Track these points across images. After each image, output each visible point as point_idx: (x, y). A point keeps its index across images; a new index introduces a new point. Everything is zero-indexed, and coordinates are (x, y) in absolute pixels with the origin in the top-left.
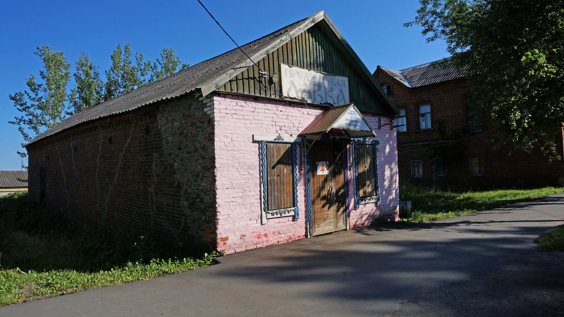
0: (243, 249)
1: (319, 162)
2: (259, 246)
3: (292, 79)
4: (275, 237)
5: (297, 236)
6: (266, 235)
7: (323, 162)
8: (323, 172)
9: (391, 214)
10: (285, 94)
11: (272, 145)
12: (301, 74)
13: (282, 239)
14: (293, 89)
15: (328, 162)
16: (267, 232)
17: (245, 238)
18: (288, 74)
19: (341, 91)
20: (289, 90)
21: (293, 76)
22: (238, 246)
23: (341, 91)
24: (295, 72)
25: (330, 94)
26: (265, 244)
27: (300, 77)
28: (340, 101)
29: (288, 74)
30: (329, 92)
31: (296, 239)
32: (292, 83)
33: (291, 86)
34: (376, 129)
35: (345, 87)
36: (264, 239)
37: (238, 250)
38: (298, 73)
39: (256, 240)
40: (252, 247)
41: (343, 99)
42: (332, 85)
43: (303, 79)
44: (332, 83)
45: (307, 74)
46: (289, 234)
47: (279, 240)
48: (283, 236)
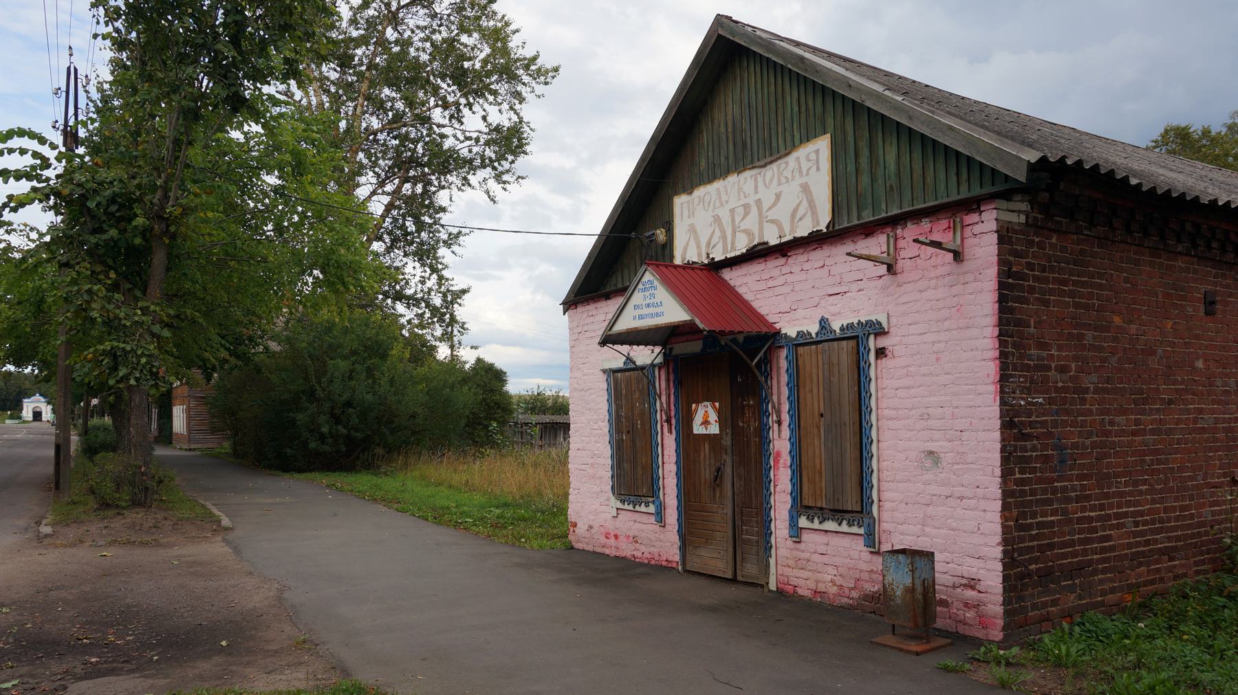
0: (590, 548)
1: (698, 403)
2: (607, 551)
5: (665, 559)
6: (616, 537)
7: (706, 403)
8: (706, 429)
9: (946, 601)
14: (692, 243)
15: (717, 404)
17: (593, 531)
18: (686, 213)
19: (806, 188)
20: (685, 249)
21: (693, 213)
23: (806, 188)
24: (696, 201)
25: (772, 215)
27: (706, 205)
28: (801, 219)
29: (686, 213)
30: (770, 209)
31: (664, 563)
34: (881, 277)
35: (818, 169)
36: (612, 541)
38: (701, 200)
39: (603, 540)
42: (779, 184)
44: (779, 180)
46: (652, 549)
47: (635, 553)
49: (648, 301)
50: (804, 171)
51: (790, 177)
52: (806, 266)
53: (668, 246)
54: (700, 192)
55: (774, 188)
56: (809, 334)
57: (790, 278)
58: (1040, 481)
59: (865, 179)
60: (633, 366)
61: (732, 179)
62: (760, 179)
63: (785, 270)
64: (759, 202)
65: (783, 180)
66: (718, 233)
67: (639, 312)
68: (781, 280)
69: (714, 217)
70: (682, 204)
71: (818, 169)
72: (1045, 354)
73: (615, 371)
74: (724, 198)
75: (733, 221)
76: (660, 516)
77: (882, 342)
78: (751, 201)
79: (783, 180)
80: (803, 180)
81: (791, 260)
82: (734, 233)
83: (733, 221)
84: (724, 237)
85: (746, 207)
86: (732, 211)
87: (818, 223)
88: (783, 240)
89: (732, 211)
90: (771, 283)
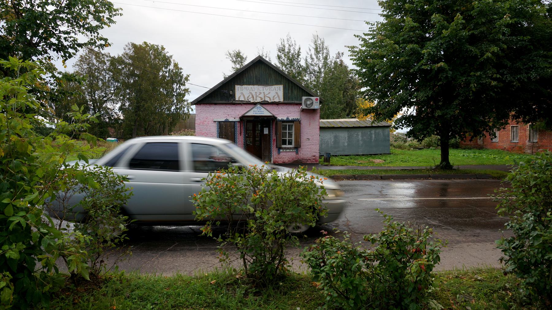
10: (237, 99)
12: (248, 88)
20: (239, 97)
23: (277, 93)
32: (242, 93)
45: (251, 88)
53: (233, 96)
54: (244, 86)
55: (268, 91)
59: (290, 94)
61: (256, 86)
62: (264, 89)
64: (264, 93)
66: (251, 96)
67: (254, 112)
73: (219, 122)
74: (253, 89)
75: (256, 95)
78: (262, 92)
82: (256, 96)
83: (256, 95)
84: (253, 97)
85: (260, 93)
86: (256, 93)
89: (256, 93)
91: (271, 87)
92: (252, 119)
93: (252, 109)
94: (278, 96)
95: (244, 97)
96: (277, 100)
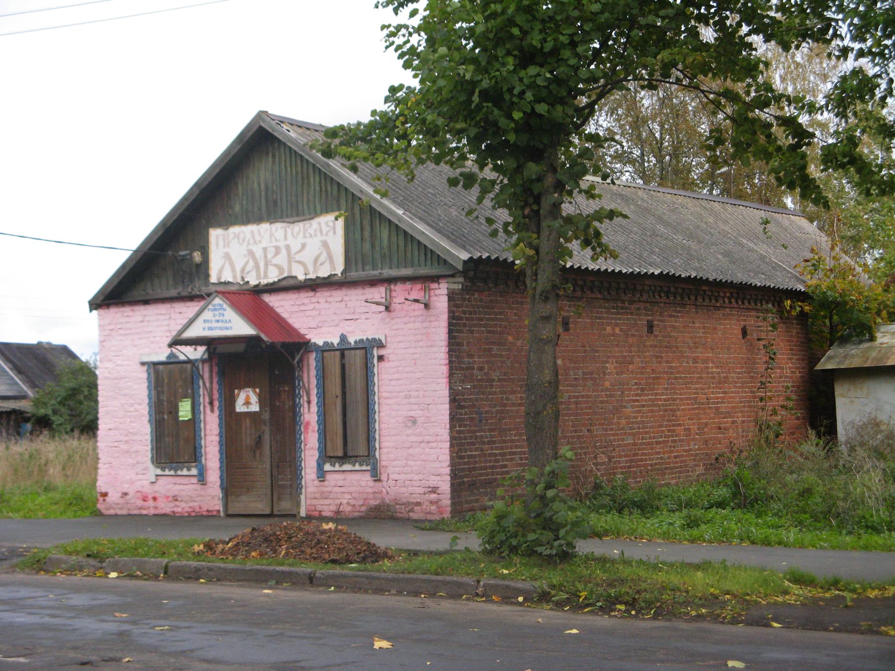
0: (124, 512)
1: (240, 388)
2: (144, 512)
3: (226, 250)
4: (171, 505)
5: (205, 509)
6: (155, 499)
7: (247, 389)
8: (248, 408)
9: (420, 503)
10: (213, 279)
11: (161, 367)
12: (242, 236)
13: (179, 510)
14: (227, 267)
15: (258, 390)
16: (157, 495)
17: (128, 497)
18: (221, 243)
19: (325, 244)
20: (221, 271)
21: (228, 244)
22: (119, 506)
23: (325, 244)
24: (232, 236)
25: (298, 257)
26: (152, 512)
27: (241, 241)
28: (322, 264)
29: (221, 243)
30: (296, 253)
31: (205, 513)
32: (227, 257)
33: (224, 264)
34: (381, 312)
35: (335, 233)
36: (151, 503)
37: (119, 512)
38: (237, 236)
39: (140, 503)
40: (136, 512)
41: (328, 261)
42: (305, 237)
43: (245, 244)
44: (304, 234)
46: (192, 504)
47: (175, 509)
48: (183, 505)
49: (217, 318)
50: (324, 233)
51: (313, 234)
52: (330, 299)
53: (203, 268)
54: (235, 230)
55: (301, 239)
56: (332, 344)
57: (317, 306)
58: (469, 431)
59: (367, 246)
60: (176, 360)
61: (265, 227)
62: (289, 231)
63: (314, 300)
64: (288, 248)
65: (308, 235)
66: (251, 263)
67: (208, 325)
68: (311, 307)
69: (248, 250)
70: (217, 236)
71: (335, 233)
72: (471, 360)
73: (155, 364)
74: (258, 238)
75: (266, 257)
76: (202, 478)
77: (382, 352)
78: (282, 244)
79: (308, 235)
80: (324, 238)
81: (318, 294)
82: (266, 265)
83: (266, 257)
84: (257, 267)
85: (278, 250)
86: (265, 249)
87: (335, 269)
88: (308, 277)
89: (265, 249)
90: (303, 308)
91: (307, 223)
92: (240, 348)
93: (198, 315)
94: (330, 257)
95: (233, 270)
96: (324, 272)
